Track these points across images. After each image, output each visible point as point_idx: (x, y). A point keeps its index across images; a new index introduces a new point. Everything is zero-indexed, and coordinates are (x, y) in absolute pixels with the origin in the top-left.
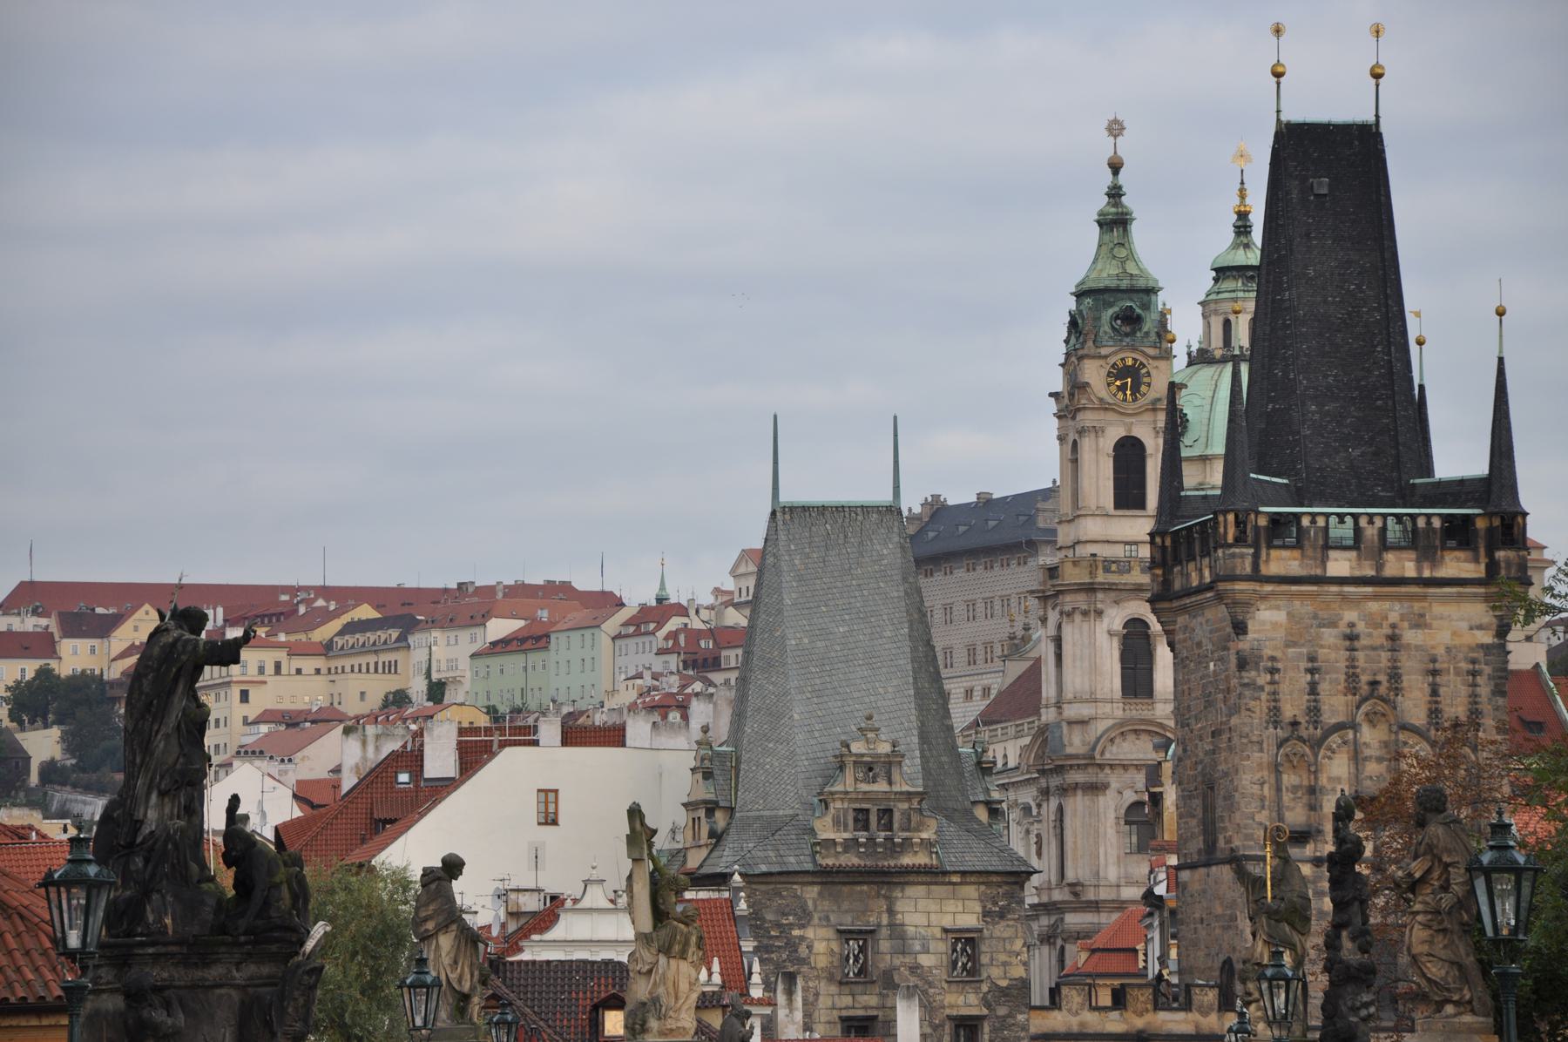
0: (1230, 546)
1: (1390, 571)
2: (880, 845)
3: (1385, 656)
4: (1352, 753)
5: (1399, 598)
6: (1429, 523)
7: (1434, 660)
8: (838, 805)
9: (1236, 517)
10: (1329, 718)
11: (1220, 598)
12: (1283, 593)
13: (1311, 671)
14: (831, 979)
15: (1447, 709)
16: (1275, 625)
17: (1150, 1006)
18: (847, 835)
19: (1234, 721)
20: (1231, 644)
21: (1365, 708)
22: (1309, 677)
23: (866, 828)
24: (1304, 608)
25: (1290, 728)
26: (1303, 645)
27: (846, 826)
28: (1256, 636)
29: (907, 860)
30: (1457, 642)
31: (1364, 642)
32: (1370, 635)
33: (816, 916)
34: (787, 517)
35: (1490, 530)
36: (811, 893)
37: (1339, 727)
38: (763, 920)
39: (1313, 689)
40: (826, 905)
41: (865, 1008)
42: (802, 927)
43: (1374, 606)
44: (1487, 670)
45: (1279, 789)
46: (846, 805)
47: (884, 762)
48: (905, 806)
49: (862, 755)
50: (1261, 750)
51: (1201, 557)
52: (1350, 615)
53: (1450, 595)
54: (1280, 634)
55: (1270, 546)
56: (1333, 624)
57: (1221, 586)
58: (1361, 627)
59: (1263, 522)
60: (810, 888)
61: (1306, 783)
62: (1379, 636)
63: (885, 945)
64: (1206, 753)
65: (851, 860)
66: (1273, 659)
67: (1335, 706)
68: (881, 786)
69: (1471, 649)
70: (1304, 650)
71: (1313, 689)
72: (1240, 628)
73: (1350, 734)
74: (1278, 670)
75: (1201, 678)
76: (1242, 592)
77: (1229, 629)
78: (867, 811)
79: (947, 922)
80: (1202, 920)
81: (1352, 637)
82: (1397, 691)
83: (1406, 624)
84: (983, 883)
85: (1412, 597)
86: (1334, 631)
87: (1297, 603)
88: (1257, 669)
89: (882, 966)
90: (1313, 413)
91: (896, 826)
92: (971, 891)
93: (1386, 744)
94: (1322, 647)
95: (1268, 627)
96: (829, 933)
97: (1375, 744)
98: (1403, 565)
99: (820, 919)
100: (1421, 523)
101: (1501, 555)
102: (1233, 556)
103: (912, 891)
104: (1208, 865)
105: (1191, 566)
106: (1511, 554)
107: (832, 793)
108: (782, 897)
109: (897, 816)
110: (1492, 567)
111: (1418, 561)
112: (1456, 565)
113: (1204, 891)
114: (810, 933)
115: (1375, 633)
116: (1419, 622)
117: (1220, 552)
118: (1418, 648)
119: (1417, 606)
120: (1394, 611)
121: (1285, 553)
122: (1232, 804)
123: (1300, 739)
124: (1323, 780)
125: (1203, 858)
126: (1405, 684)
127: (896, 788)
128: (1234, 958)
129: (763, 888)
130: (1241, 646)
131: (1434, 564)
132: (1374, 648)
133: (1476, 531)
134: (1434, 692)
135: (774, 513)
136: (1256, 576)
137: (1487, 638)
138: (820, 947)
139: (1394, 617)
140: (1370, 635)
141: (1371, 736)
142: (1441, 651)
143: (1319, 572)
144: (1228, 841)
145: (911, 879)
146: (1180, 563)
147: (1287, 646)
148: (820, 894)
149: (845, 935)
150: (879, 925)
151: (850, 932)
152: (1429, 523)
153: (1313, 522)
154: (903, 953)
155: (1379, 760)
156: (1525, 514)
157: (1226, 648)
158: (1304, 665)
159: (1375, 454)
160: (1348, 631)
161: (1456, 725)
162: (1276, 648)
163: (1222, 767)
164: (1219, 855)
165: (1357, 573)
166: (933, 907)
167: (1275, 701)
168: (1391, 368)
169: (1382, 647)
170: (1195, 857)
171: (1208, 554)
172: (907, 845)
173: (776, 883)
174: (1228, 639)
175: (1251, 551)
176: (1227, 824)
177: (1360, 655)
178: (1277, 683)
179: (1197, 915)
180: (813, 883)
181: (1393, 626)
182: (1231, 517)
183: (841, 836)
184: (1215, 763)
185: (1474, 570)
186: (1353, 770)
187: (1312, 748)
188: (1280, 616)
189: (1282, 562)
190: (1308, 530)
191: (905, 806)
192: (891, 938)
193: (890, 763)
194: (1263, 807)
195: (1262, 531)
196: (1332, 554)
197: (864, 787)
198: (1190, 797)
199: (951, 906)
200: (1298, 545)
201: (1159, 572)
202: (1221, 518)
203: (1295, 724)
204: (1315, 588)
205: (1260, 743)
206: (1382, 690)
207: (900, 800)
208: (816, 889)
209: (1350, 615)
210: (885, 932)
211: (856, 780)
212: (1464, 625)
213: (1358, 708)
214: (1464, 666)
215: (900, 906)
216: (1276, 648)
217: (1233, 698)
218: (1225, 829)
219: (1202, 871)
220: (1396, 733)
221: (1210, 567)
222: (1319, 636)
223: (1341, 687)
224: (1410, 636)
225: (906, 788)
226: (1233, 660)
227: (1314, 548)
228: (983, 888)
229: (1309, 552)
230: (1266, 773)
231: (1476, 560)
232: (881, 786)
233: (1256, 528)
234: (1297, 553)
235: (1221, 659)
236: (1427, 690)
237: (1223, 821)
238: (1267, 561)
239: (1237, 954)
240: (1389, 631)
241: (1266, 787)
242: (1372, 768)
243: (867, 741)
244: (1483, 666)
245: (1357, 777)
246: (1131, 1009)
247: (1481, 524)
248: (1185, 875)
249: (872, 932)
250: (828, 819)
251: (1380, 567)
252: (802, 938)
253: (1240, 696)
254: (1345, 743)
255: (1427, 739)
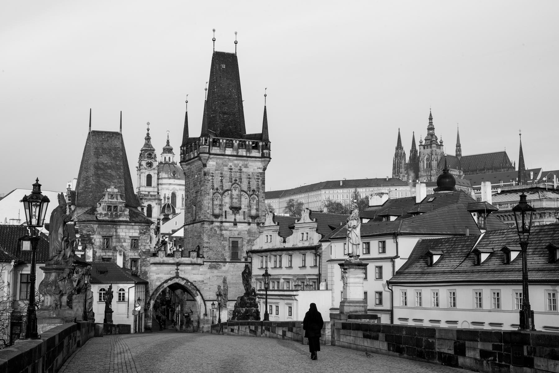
0: (203, 145)
1: (240, 154)
2: (114, 215)
3: (238, 174)
4: (230, 197)
5: (242, 160)
6: (249, 143)
7: (249, 175)
8: (104, 204)
9: (205, 138)
10: (225, 188)
11: (200, 159)
12: (215, 158)
13: (222, 177)
14: (100, 248)
15: (252, 187)
16: (213, 165)
17: (180, 256)
18: (106, 212)
19: (202, 188)
20: (202, 170)
21: (233, 186)
22: (221, 178)
23: (110, 210)
24: (220, 161)
25: (216, 190)
26: (219, 170)
27: (105, 210)
28: (209, 168)
29: (121, 219)
30: (254, 171)
31: (233, 170)
32: (235, 169)
33: (97, 232)
34: (93, 134)
35: (263, 145)
36: (95, 226)
37: (227, 190)
38: (83, 233)
39: (222, 181)
40: (99, 230)
41: (109, 256)
42: (93, 235)
43: (236, 162)
44: (261, 178)
45: (213, 205)
46: (105, 204)
47: (116, 194)
48: (121, 205)
49: (110, 192)
50: (209, 195)
51: (195, 150)
52: (230, 164)
53: (253, 160)
54: (214, 168)
55: (213, 146)
56: (226, 166)
57: (201, 155)
58: (233, 167)
59: (211, 140)
60: (95, 225)
61: (219, 203)
62: (237, 169)
63: (114, 240)
64: (194, 197)
65: (106, 218)
66: (213, 173)
67: (227, 185)
68: (115, 200)
69: (258, 173)
70: (220, 172)
71: (222, 181)
72: (205, 165)
73: (230, 192)
74: (213, 176)
75: (193, 180)
76: (206, 156)
77: (202, 166)
78: (111, 206)
79: (131, 235)
80: (191, 237)
81: (231, 169)
82: (241, 182)
83: (243, 167)
84: (139, 225)
85: (244, 160)
86: (227, 167)
87: (218, 160)
88: (209, 176)
89: (113, 245)
90: (222, 117)
91: (118, 210)
92: (137, 227)
93: (238, 195)
94: (224, 171)
95: (211, 166)
96: (100, 237)
97: (235, 195)
98: (243, 152)
99: (98, 233)
100: (247, 143)
101: (265, 151)
102: (204, 148)
103: (121, 227)
104: (193, 223)
105: (191, 153)
106: (267, 151)
107: (102, 201)
108: (88, 227)
109: (119, 208)
110: (263, 154)
111: (246, 152)
112: (255, 153)
113: (192, 230)
114: (95, 236)
115: (236, 168)
116: (246, 166)
117: (201, 147)
118: (245, 172)
119: (246, 162)
120: (241, 163)
121: (216, 148)
122: (201, 208)
123: (218, 193)
124: (223, 203)
125: (192, 222)
126: (242, 181)
127: (119, 201)
128: (200, 246)
129: (83, 224)
130: (205, 170)
131: (250, 153)
132: (236, 172)
133: (259, 146)
134: (249, 183)
135: (89, 133)
136: (209, 153)
137: (261, 171)
138: (97, 240)
139: (240, 165)
140: (235, 169)
141: (235, 193)
142: (251, 173)
143: (224, 153)
144: (200, 217)
145: (122, 223)
146: (188, 153)
147: (216, 170)
148: (98, 227)
149: (104, 237)
150: (113, 235)
151: (105, 236)
152: (249, 143)
153: (223, 141)
154: (119, 242)
155: (236, 199)
156: (270, 142)
157: (200, 171)
158: (220, 175)
159: (235, 128)
160: (230, 168)
161: (254, 191)
162: (213, 171)
163: (199, 200)
164: (196, 221)
165: (232, 154)
166: (127, 231)
167: (213, 183)
168: (239, 108)
169: (238, 172)
170: (189, 223)
171: (196, 149)
172: (120, 215)
173: (86, 223)
174: (201, 169)
175: (208, 147)
176: (199, 213)
177: (232, 173)
178: (213, 179)
179: (190, 236)
180: (96, 224)
181: (240, 167)
182: (204, 138)
183: (104, 212)
184: (196, 199)
185: (259, 155)
186: (230, 201)
187: (221, 195)
188: (214, 163)
189: (215, 150)
190: (221, 143)
191: (121, 205)
192: (116, 238)
193: (117, 194)
194: (209, 209)
195: (211, 143)
196: (227, 149)
197: (110, 200)
198: (188, 209)
199: (132, 231)
200: (219, 146)
201: (182, 156)
202: (201, 139)
203: (217, 189)
204: (223, 157)
205: (209, 194)
206: (237, 182)
207: (120, 204)
208: (97, 225)
209: (230, 164)
210: (114, 237)
211: (108, 198)
212: (256, 168)
213: (232, 186)
214: (256, 177)
215: (118, 231)
216: (213, 171)
217: (202, 183)
218: (199, 215)
219: (192, 225)
220: (240, 192)
221: (197, 152)
222: (223, 169)
223: (228, 181)
224: (244, 170)
225: (121, 201)
226: (203, 173)
227: (223, 147)
228: (140, 227)
229: (222, 148)
230: (210, 201)
231: (259, 152)
232: (115, 200)
233: (209, 141)
234: (219, 148)
235: (199, 174)
236: (247, 182)
237: (198, 212)
238: (212, 150)
239: (201, 244)
240: (239, 168)
241: (210, 204)
242: (234, 200)
243: (112, 189)
244: (260, 177)
245: (232, 202)
246: (175, 257)
247: (261, 144)
248: (187, 227)
249: (111, 237)
250: (101, 208)
251: (238, 153)
252: (93, 238)
253: (204, 182)
254: (228, 194)
255: (247, 194)
